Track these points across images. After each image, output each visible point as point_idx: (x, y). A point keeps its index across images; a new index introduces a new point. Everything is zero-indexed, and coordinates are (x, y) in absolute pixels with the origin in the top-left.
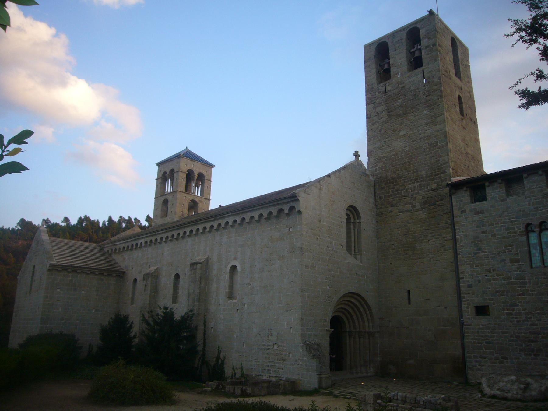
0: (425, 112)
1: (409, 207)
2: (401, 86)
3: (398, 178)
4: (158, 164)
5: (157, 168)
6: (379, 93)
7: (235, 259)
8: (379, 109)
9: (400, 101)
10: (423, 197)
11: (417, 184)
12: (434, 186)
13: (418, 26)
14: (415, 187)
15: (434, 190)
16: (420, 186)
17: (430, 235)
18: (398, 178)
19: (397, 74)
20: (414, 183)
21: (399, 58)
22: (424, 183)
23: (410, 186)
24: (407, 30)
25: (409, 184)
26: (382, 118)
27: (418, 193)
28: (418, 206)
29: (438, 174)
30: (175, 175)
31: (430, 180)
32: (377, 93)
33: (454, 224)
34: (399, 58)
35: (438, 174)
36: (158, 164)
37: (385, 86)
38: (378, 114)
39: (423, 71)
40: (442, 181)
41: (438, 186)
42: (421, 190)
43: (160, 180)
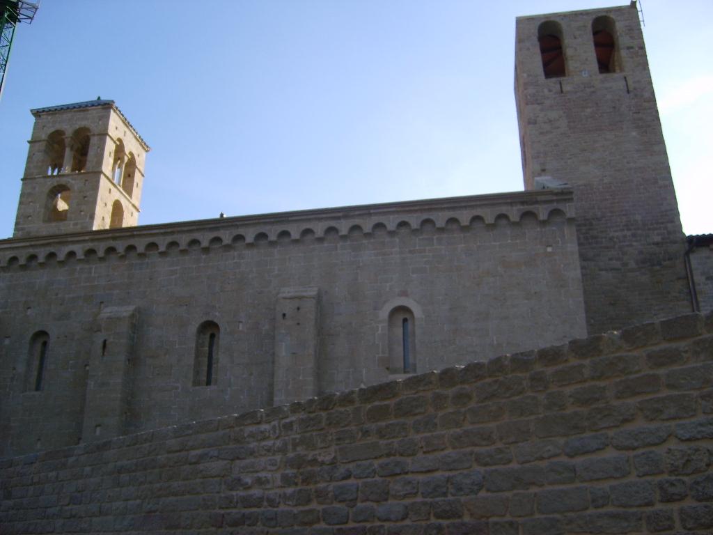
0: (634, 134)
1: (617, 264)
2: (588, 90)
3: (593, 219)
4: (37, 113)
5: (33, 119)
6: (550, 91)
7: (404, 294)
8: (553, 115)
9: (589, 110)
10: (641, 252)
11: (629, 233)
12: (658, 239)
13: (612, 16)
14: (625, 236)
15: (657, 244)
16: (634, 235)
17: (656, 308)
18: (593, 219)
19: (581, 71)
20: (623, 230)
21: (581, 52)
22: (639, 232)
23: (617, 234)
24: (594, 17)
25: (616, 231)
26: (558, 128)
27: (631, 245)
28: (632, 265)
29: (662, 223)
30: (94, 141)
31: (649, 229)
32: (546, 91)
33: (695, 294)
34: (581, 52)
35: (662, 223)
36: (37, 113)
37: (560, 83)
38: (550, 121)
39: (625, 78)
40: (669, 233)
41: (663, 239)
42: (636, 241)
43: (42, 146)
